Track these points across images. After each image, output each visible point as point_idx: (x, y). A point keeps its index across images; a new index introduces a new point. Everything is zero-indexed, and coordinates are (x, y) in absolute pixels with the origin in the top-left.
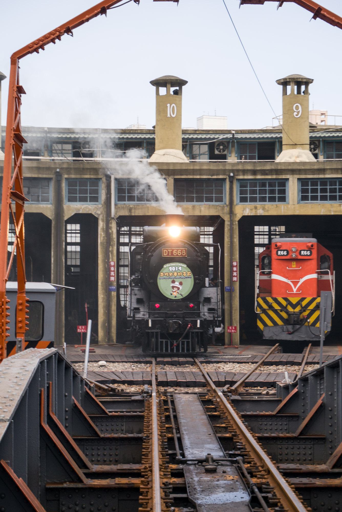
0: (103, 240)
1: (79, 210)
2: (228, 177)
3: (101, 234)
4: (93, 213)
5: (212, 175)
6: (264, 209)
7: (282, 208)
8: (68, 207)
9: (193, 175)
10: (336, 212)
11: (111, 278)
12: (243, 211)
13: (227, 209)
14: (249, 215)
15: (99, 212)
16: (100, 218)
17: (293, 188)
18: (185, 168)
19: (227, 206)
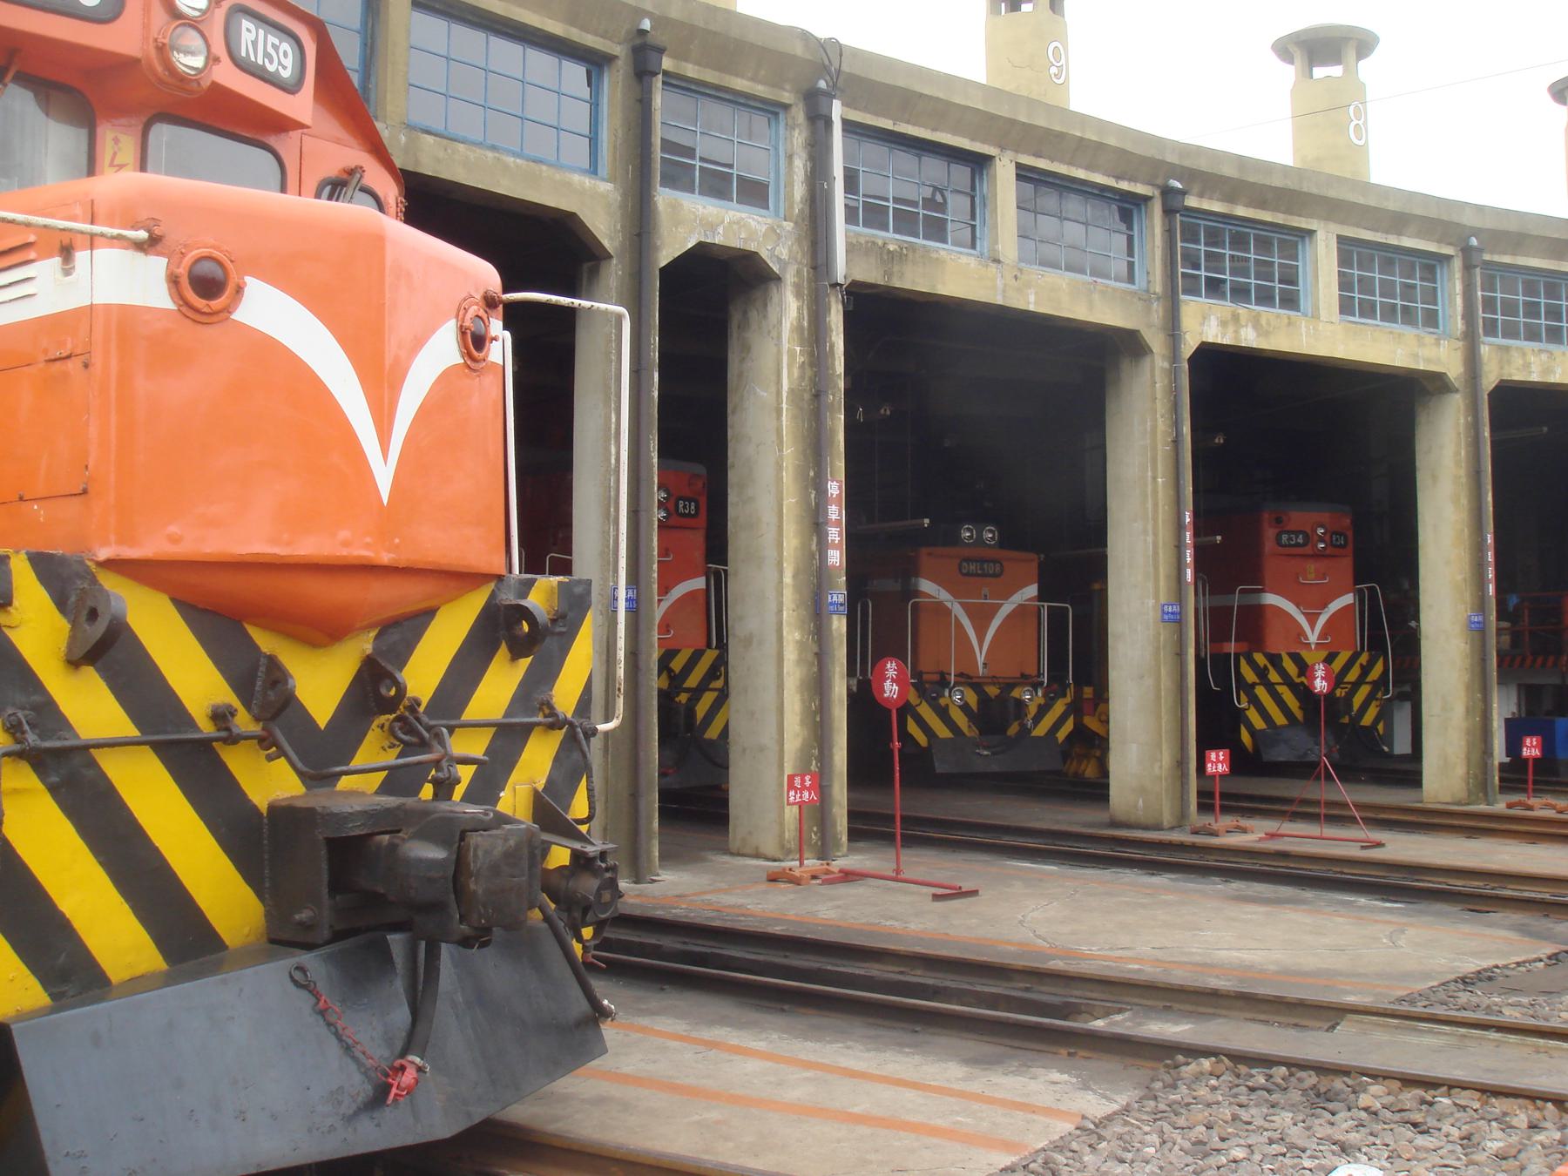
0: (802, 377)
1: (713, 227)
2: (1157, 193)
3: (791, 353)
4: (764, 254)
5: (1118, 178)
6: (1256, 325)
7: (1304, 329)
8: (675, 207)
9: (1070, 163)
10: (1428, 361)
11: (830, 552)
12: (1202, 324)
13: (1158, 311)
14: (1219, 341)
15: (784, 252)
16: (790, 278)
17: (1322, 266)
18: (1058, 128)
19: (1158, 299)
